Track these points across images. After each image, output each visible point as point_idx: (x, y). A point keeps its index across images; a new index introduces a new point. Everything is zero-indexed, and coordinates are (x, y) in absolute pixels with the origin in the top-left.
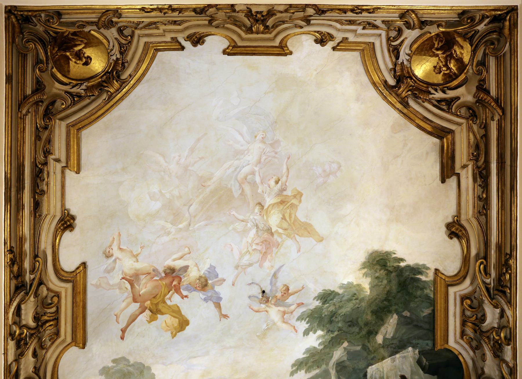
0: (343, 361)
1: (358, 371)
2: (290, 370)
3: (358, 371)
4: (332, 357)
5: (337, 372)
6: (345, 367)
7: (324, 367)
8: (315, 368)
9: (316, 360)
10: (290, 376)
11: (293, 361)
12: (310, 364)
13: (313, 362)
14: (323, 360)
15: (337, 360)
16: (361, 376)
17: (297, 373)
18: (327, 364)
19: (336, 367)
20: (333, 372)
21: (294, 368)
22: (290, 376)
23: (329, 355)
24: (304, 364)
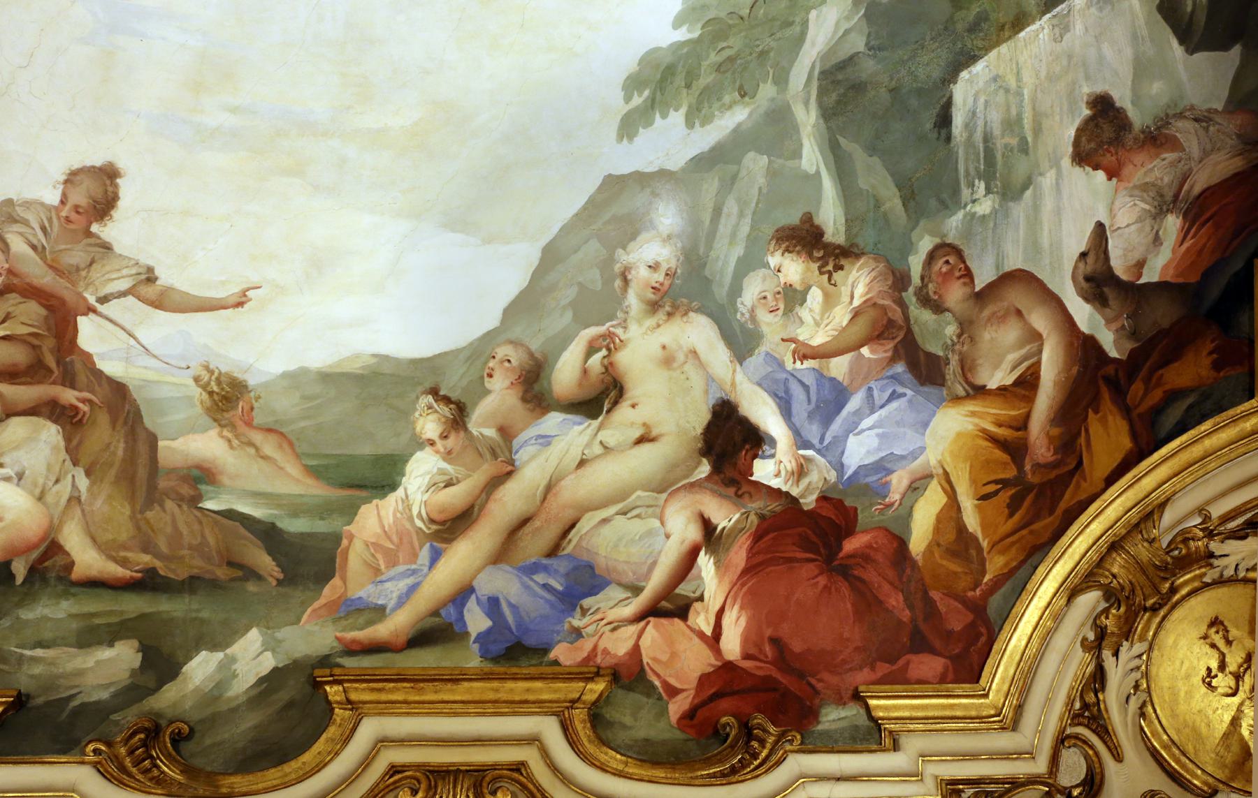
0: (851, 60)
1: (914, 102)
2: (619, 106)
3: (914, 102)
4: (801, 39)
5: (828, 114)
6: (858, 88)
7: (767, 91)
8: (727, 99)
9: (731, 59)
10: (620, 138)
11: (629, 62)
12: (706, 79)
13: (719, 68)
14: (763, 54)
15: (824, 57)
16: (929, 125)
17: (649, 123)
18: (781, 80)
19: (822, 92)
20: (807, 118)
21: (637, 100)
22: (620, 138)
23: (788, 32)
24: (680, 80)
